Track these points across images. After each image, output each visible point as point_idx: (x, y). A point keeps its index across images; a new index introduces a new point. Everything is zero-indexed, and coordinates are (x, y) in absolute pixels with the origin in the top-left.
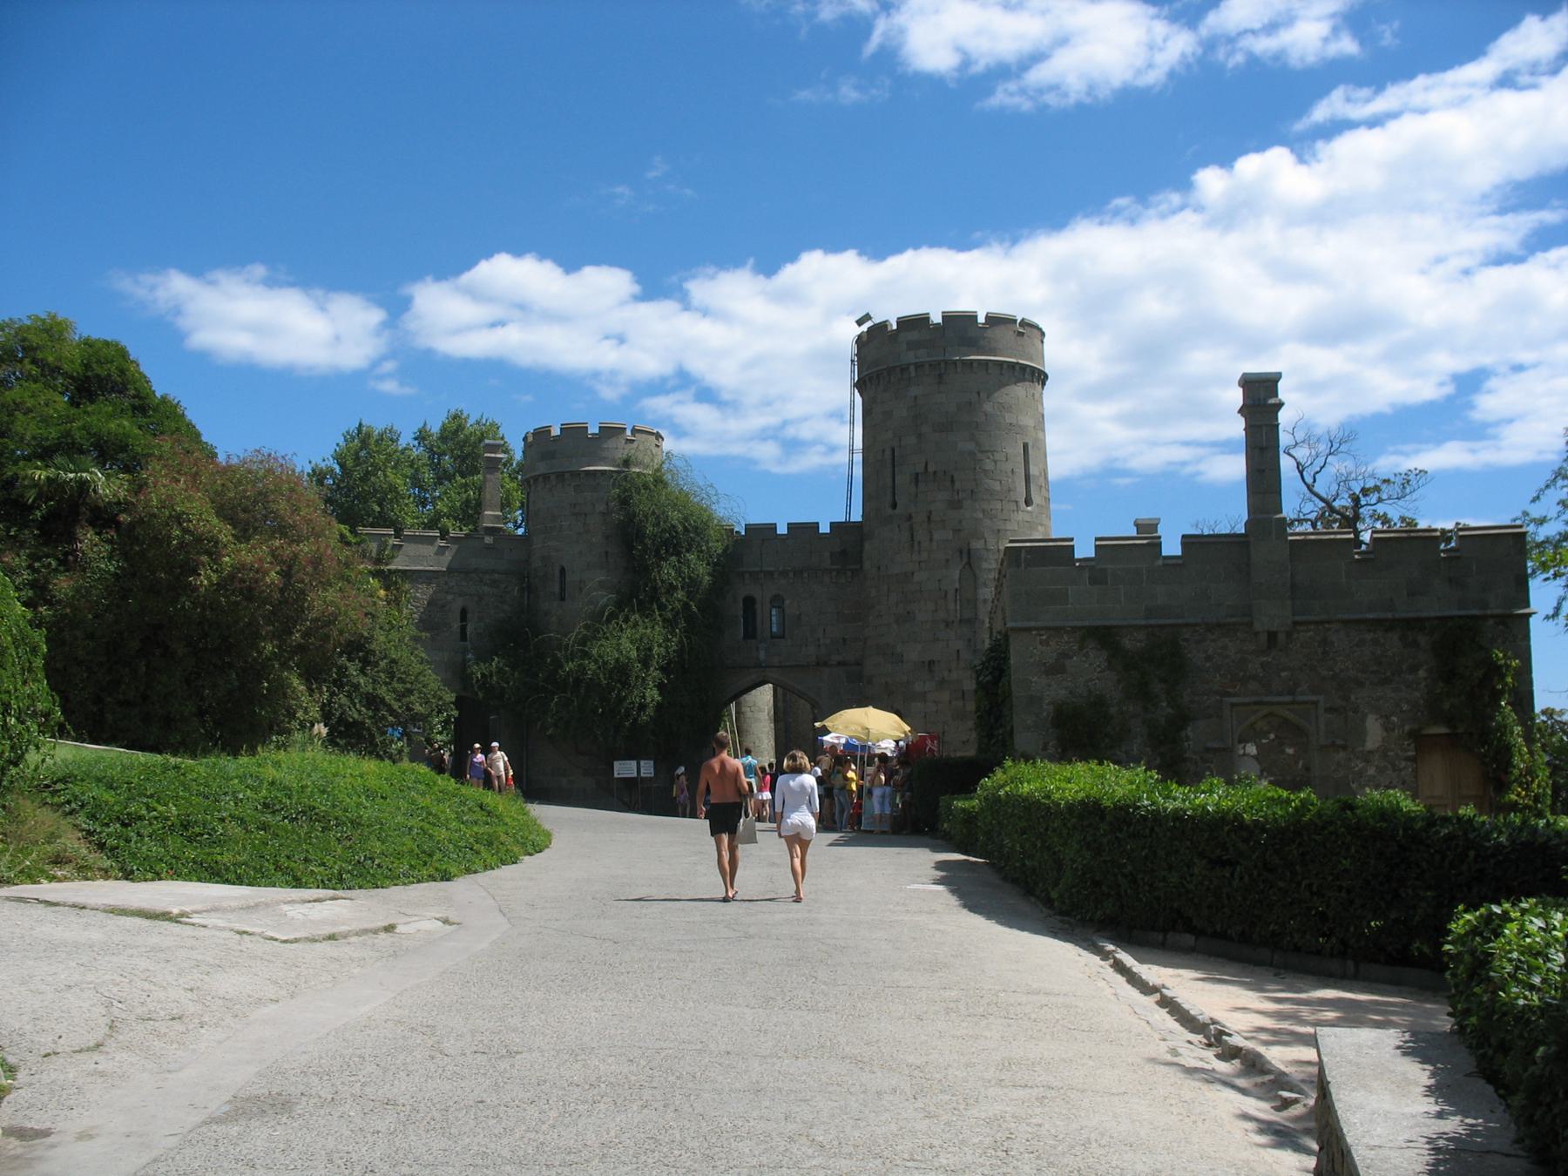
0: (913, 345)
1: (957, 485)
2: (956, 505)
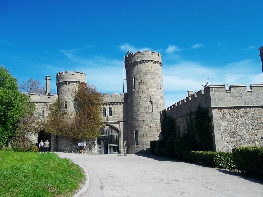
1: (148, 85)
2: (148, 89)
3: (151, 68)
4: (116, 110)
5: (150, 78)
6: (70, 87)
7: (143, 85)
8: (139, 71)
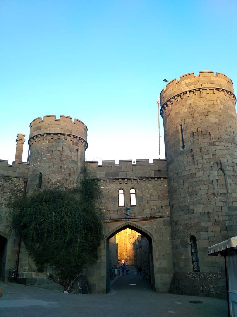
0: (187, 85)
1: (212, 136)
2: (212, 144)
5: (216, 123)
7: (200, 137)
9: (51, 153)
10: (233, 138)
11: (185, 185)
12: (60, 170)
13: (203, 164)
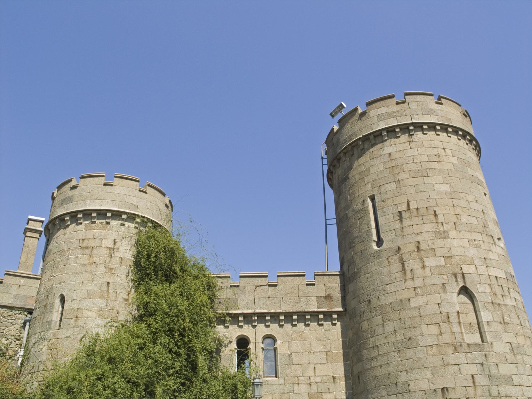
1: (441, 218)
2: (443, 235)
3: (442, 152)
4: (297, 346)
5: (446, 192)
6: (90, 234)
7: (416, 221)
8: (389, 165)
9: (88, 252)
10: (484, 224)
11: (386, 327)
12: (106, 289)
13: (424, 278)
